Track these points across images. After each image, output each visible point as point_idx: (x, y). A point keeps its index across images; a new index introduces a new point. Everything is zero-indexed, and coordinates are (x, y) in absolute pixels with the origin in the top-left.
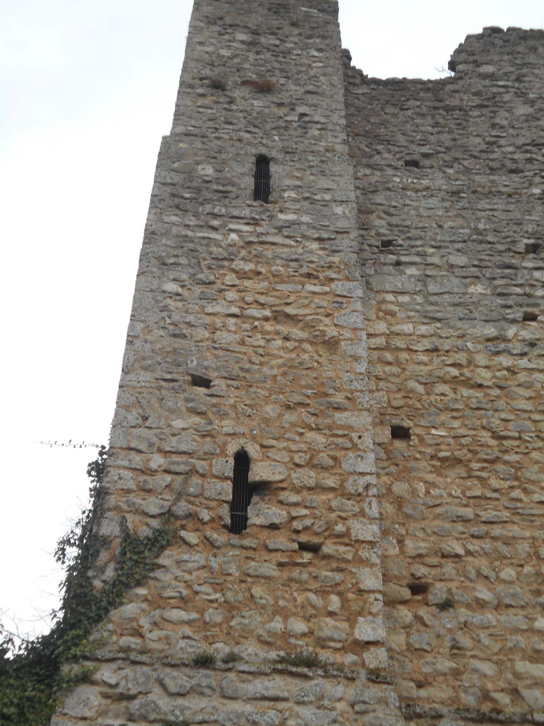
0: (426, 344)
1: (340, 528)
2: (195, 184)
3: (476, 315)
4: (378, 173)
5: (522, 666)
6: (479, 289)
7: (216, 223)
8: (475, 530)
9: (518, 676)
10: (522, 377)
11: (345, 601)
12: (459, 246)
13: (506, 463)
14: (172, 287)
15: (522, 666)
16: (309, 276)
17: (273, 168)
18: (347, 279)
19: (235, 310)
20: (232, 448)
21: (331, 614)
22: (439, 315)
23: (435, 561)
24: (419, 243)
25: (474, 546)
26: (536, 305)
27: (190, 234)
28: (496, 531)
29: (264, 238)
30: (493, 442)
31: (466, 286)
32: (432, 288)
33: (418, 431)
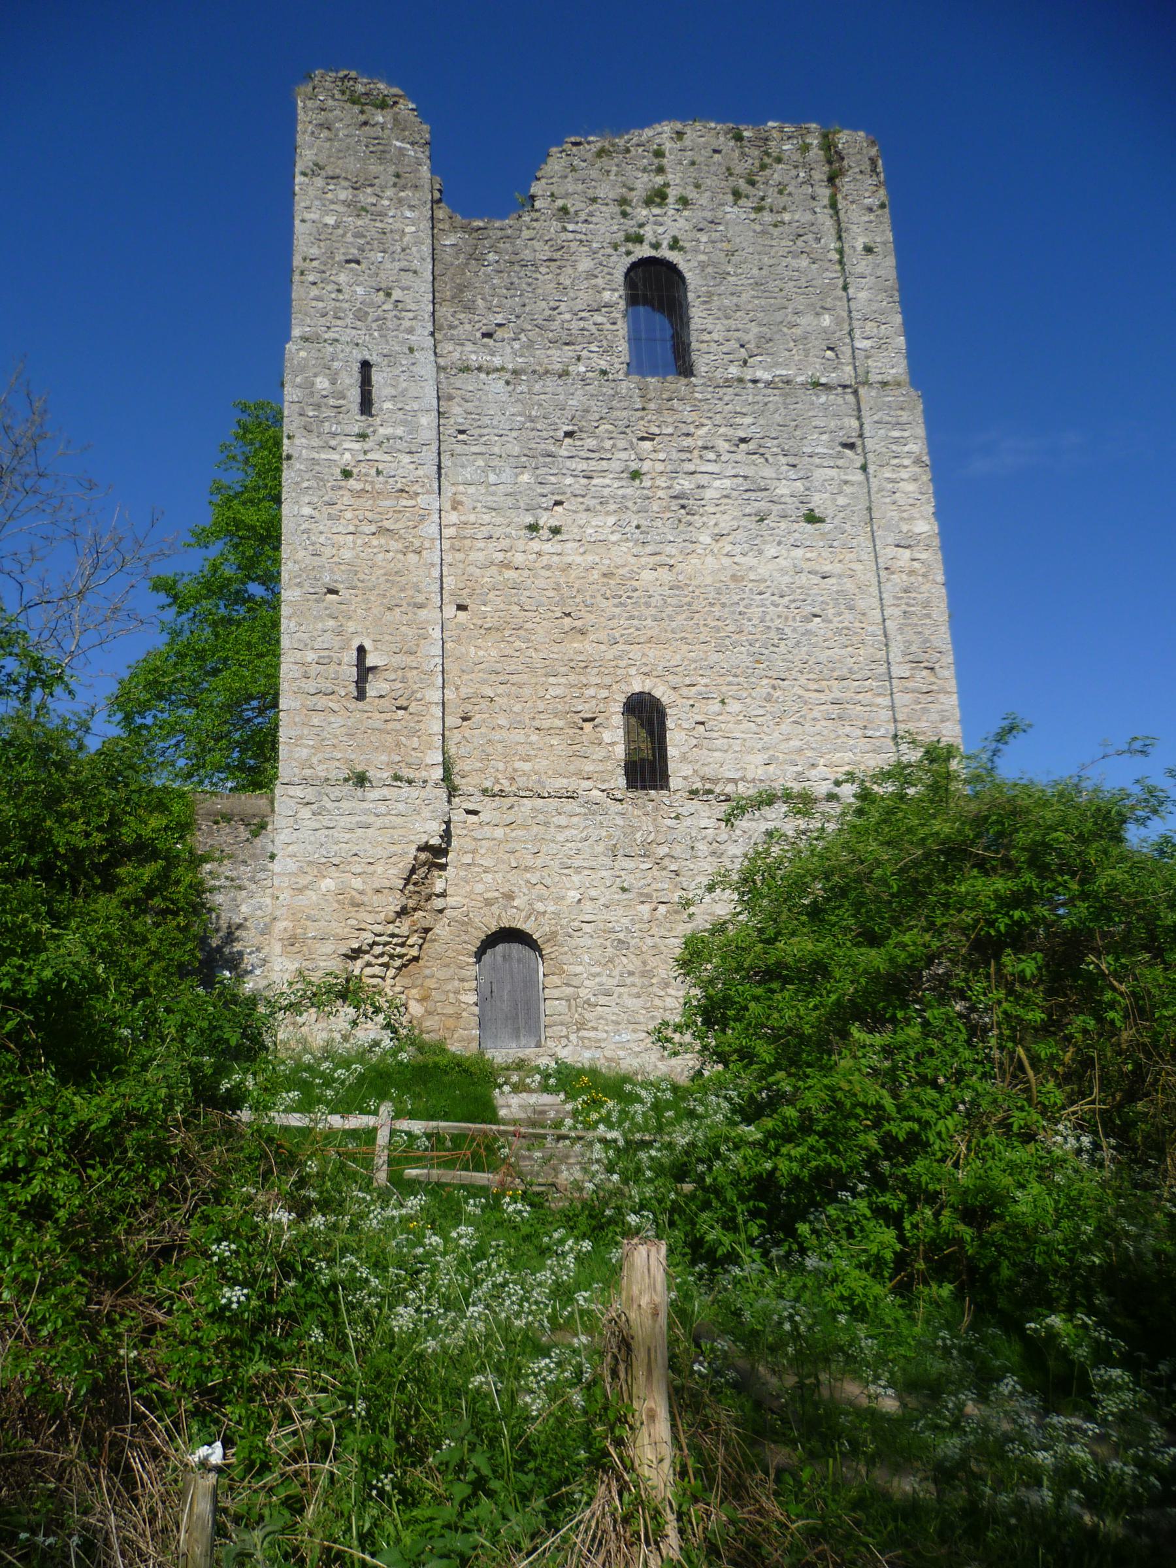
0: (485, 531)
1: (419, 696)
2: (316, 399)
3: (522, 504)
4: (459, 348)
5: (519, 765)
6: (525, 478)
7: (333, 443)
8: (501, 678)
9: (515, 770)
10: (545, 560)
12: (515, 434)
14: (307, 511)
15: (519, 765)
16: (402, 491)
17: (376, 377)
18: (428, 492)
19: (352, 529)
20: (355, 645)
22: (494, 505)
24: (485, 431)
25: (501, 689)
26: (564, 493)
27: (316, 456)
29: (369, 457)
31: (517, 475)
32: (492, 478)
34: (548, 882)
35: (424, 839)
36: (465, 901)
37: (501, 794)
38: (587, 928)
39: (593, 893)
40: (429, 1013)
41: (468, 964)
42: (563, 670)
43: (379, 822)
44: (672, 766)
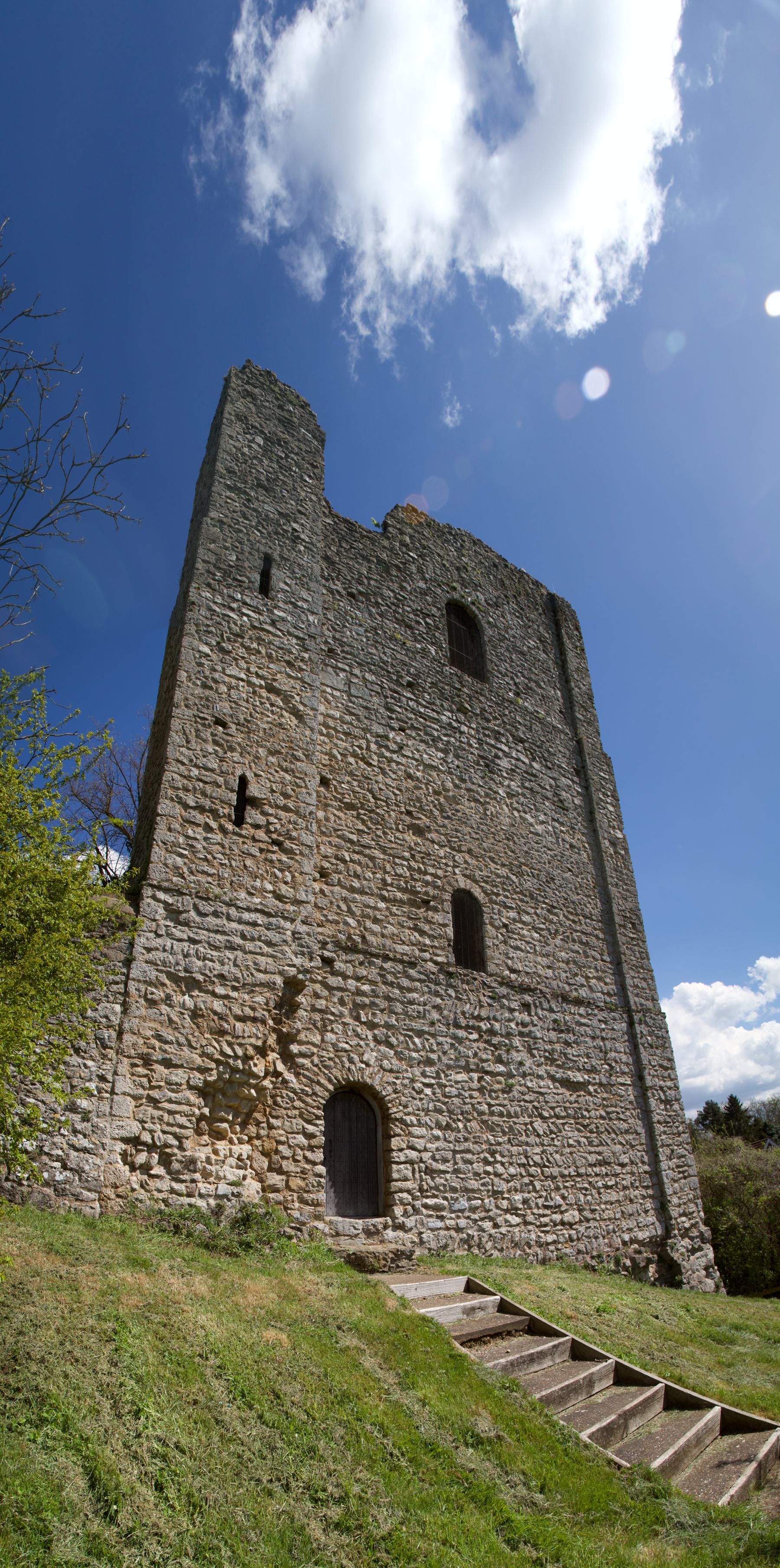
5: (369, 924)
9: (365, 929)
11: (293, 877)
13: (377, 814)
15: (369, 924)
21: (286, 883)
23: (334, 861)
25: (356, 857)
28: (367, 851)
30: (372, 800)
33: (334, 782)
34: (393, 1040)
35: (292, 971)
36: (315, 1050)
37: (353, 949)
38: (428, 1091)
39: (434, 1056)
40: (270, 1169)
41: (318, 1118)
42: (407, 854)
43: (249, 946)
44: (489, 952)
